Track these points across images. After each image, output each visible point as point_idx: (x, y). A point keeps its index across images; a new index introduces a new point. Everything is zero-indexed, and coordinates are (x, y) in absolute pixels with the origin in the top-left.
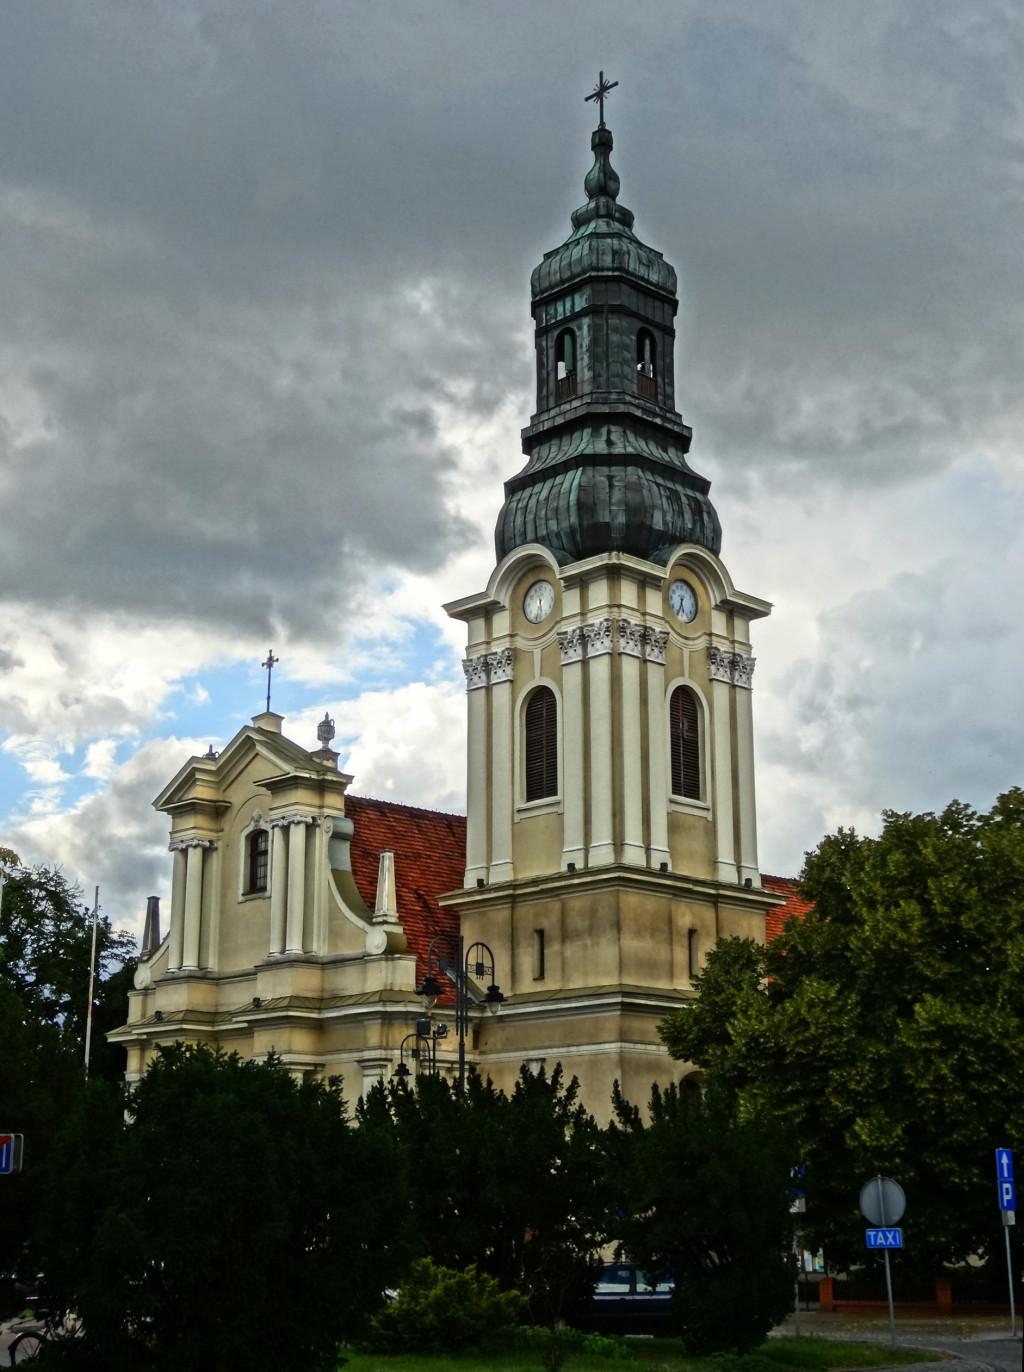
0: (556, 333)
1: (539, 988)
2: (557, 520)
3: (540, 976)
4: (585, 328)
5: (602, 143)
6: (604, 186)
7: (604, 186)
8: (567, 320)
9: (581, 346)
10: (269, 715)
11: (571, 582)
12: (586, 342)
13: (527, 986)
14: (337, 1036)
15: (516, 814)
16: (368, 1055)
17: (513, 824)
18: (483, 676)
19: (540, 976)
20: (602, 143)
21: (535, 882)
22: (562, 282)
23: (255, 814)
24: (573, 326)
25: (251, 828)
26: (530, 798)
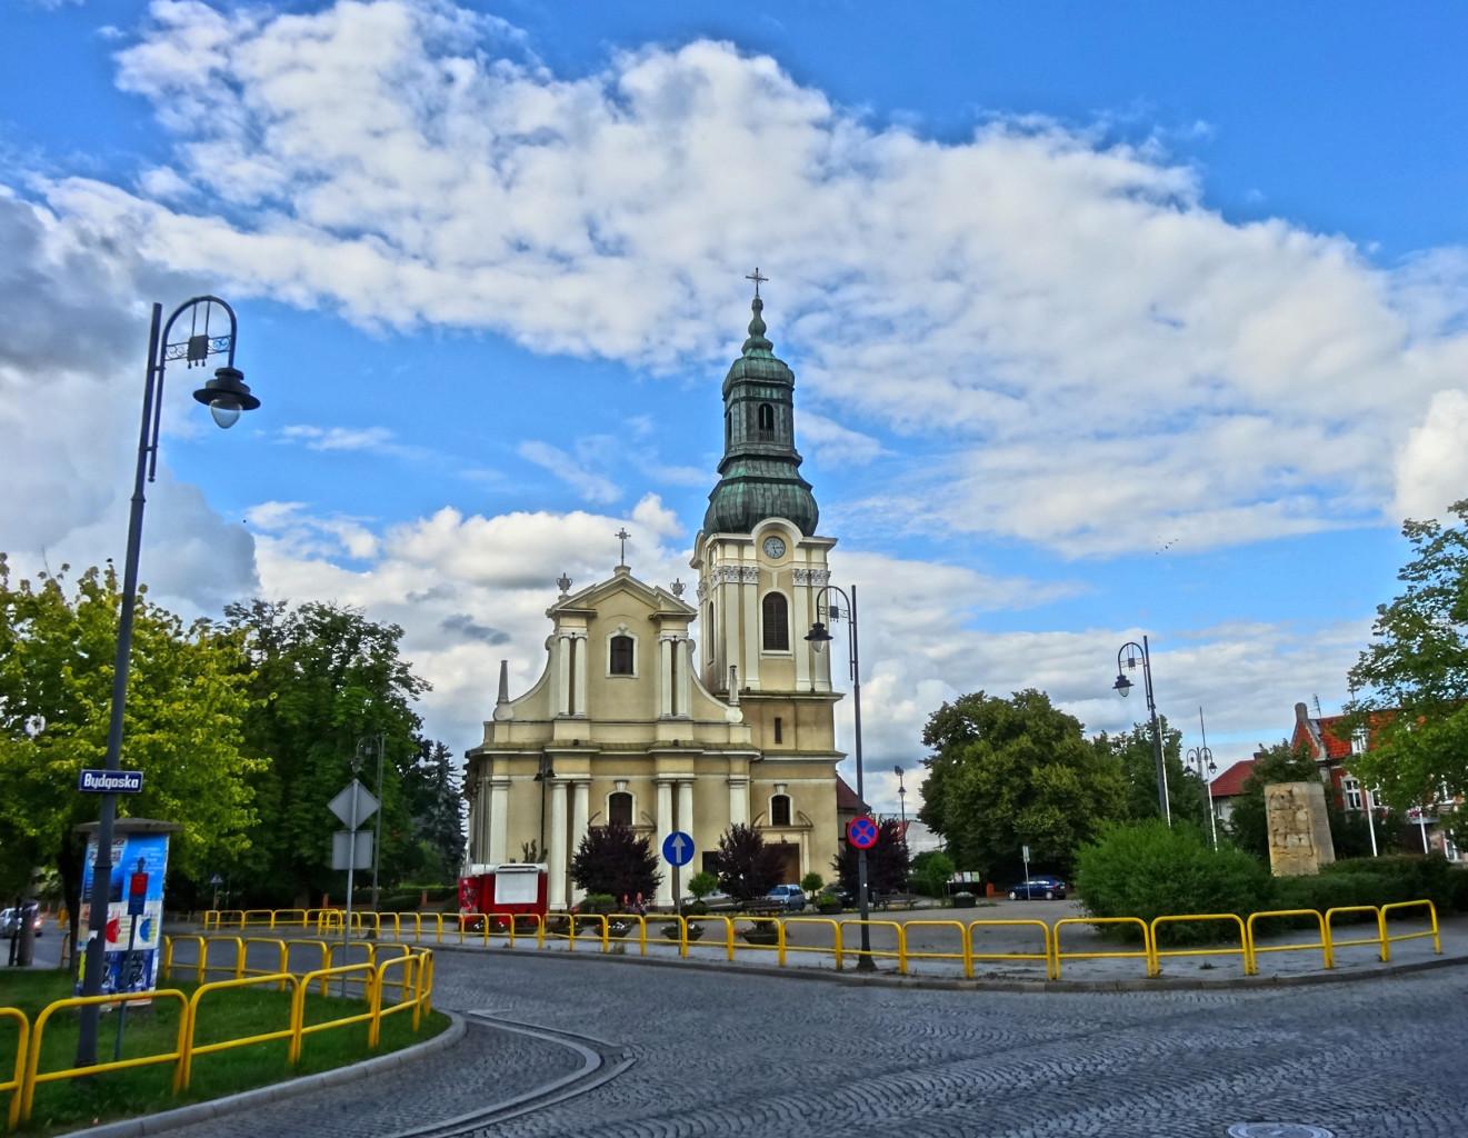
0: (760, 403)
1: (779, 747)
3: (778, 739)
5: (758, 306)
6: (758, 328)
7: (758, 328)
8: (766, 399)
10: (623, 567)
11: (801, 545)
12: (781, 417)
13: (770, 745)
14: (704, 765)
19: (778, 739)
20: (758, 306)
21: (788, 695)
23: (623, 626)
24: (773, 405)
25: (617, 633)
26: (765, 648)
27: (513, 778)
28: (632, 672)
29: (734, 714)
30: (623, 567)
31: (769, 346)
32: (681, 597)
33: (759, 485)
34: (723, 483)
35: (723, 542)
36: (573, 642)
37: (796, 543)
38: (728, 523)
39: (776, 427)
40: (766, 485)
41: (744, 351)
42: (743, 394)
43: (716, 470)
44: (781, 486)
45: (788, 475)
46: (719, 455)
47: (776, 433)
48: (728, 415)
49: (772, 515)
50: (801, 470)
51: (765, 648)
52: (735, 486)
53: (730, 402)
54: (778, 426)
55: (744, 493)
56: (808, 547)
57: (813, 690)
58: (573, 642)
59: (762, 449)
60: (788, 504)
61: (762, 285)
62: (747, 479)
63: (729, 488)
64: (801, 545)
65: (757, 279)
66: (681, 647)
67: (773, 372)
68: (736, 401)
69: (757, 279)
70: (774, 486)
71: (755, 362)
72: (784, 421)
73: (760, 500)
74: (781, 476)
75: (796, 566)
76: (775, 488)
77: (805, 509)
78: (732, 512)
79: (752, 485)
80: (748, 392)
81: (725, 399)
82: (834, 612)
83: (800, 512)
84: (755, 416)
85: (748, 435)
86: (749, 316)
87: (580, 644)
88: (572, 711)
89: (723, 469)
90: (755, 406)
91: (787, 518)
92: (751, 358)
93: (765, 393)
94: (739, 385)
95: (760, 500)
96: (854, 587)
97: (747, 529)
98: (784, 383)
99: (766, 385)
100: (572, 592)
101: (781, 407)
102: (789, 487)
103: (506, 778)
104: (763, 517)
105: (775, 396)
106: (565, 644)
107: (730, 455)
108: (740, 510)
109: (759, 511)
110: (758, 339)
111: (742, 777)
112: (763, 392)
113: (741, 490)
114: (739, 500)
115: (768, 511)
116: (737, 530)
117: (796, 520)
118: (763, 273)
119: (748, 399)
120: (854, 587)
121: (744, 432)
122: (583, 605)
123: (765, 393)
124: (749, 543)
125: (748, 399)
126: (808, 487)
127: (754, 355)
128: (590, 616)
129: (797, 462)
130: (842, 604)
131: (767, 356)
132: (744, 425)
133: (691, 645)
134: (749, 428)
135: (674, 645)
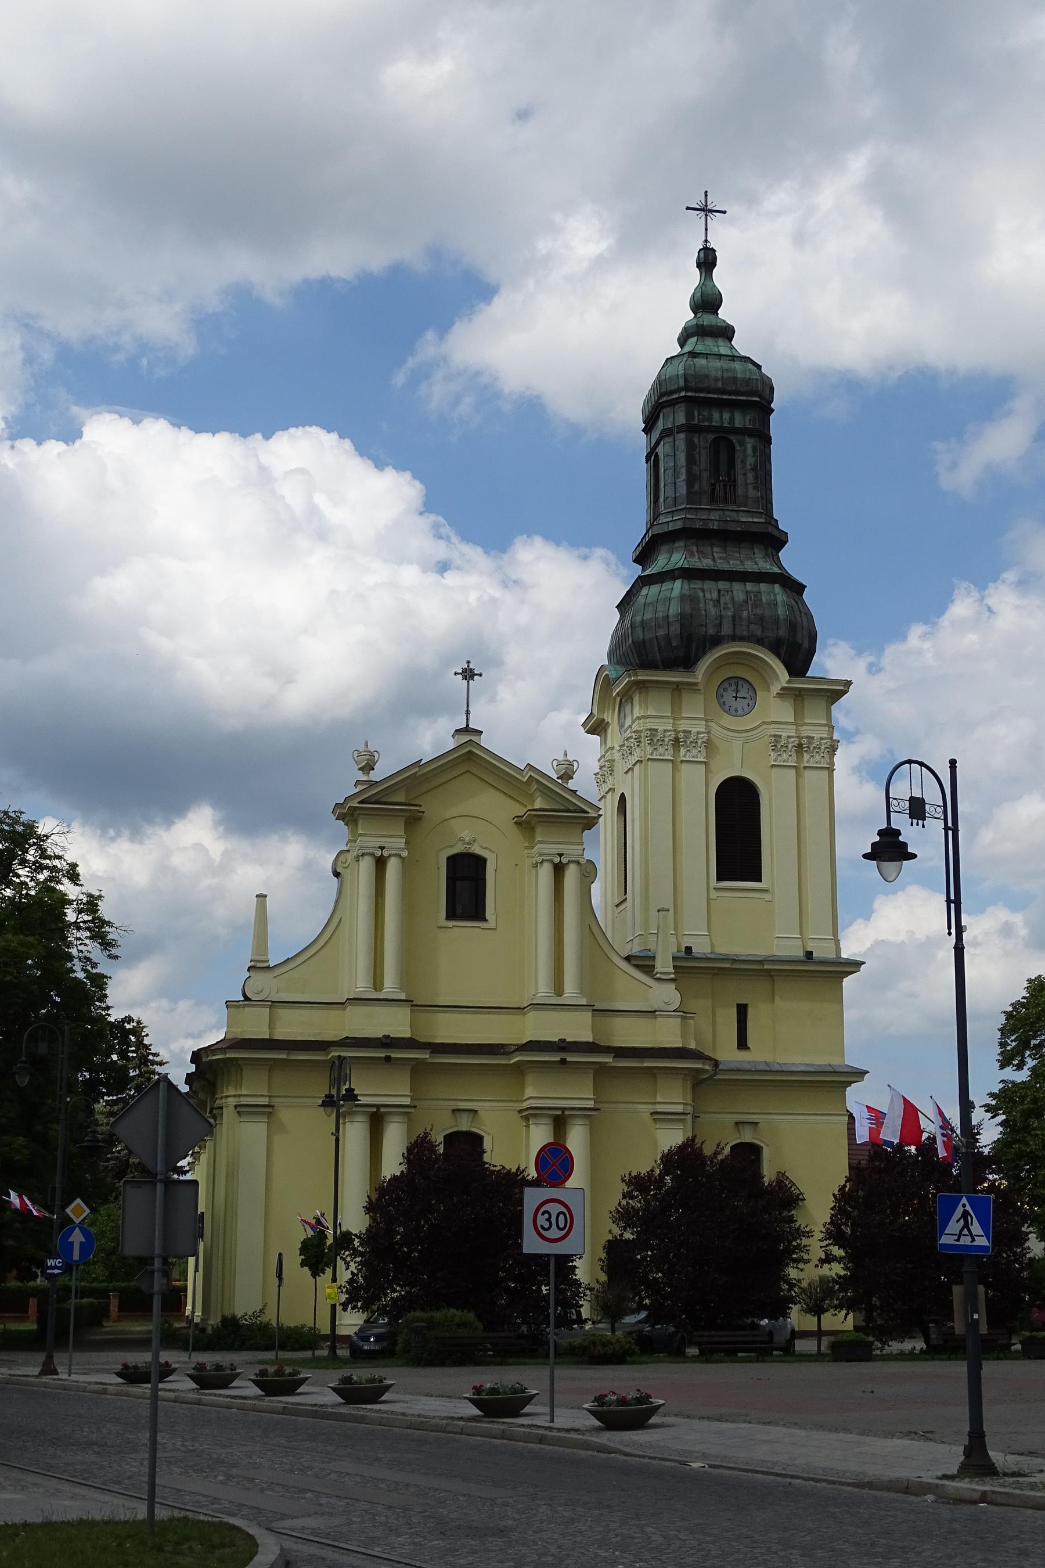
0: (711, 437)
2: (763, 627)
3: (742, 1043)
4: (749, 446)
5: (707, 261)
6: (707, 302)
7: (707, 302)
8: (720, 429)
9: (743, 462)
10: (467, 730)
11: (786, 693)
12: (750, 461)
15: (714, 894)
16: (660, 1108)
18: (670, 748)
19: (742, 1043)
20: (707, 261)
21: (761, 962)
22: (723, 392)
24: (733, 438)
27: (276, 1101)
28: (483, 919)
29: (666, 995)
30: (467, 730)
31: (727, 333)
32: (571, 785)
33: (709, 585)
34: (642, 582)
35: (642, 686)
36: (381, 863)
37: (775, 689)
38: (652, 654)
39: (740, 479)
40: (722, 585)
41: (682, 341)
42: (681, 419)
43: (631, 557)
44: (749, 586)
45: (766, 566)
46: (637, 530)
47: (740, 491)
48: (652, 457)
49: (734, 638)
50: (785, 555)
51: (719, 878)
52: (667, 586)
53: (656, 434)
54: (744, 479)
55: (682, 597)
56: (797, 697)
57: (809, 955)
58: (381, 863)
59: (713, 518)
60: (762, 618)
61: (715, 221)
62: (687, 574)
63: (655, 589)
64: (786, 693)
65: (706, 210)
66: (571, 875)
67: (735, 379)
68: (666, 433)
70: (737, 586)
71: (702, 361)
72: (754, 469)
73: (713, 611)
74: (749, 566)
75: (773, 730)
76: (739, 591)
77: (793, 626)
78: (661, 633)
79: (697, 584)
80: (689, 416)
81: (647, 430)
82: (917, 809)
83: (783, 632)
84: (704, 459)
85: (689, 493)
86: (694, 277)
87: (393, 868)
88: (377, 982)
89: (643, 557)
90: (703, 442)
91: (760, 642)
92: (693, 354)
93: (720, 418)
94: (672, 403)
95: (713, 611)
96: (953, 763)
97: (688, 663)
99: (721, 404)
100: (376, 775)
101: (750, 443)
102: (763, 587)
103: (265, 1101)
104: (716, 641)
105: (739, 422)
106: (366, 866)
107: (656, 530)
108: (675, 629)
109: (711, 631)
110: (707, 319)
111: (679, 1108)
112: (716, 415)
113: (676, 592)
114: (674, 609)
115: (727, 630)
116: (669, 664)
117: (775, 648)
118: (714, 203)
119: (690, 429)
120: (953, 763)
121: (683, 489)
122: (401, 797)
123: (720, 418)
124: (692, 687)
125: (690, 429)
126: (796, 588)
127: (700, 348)
128: (413, 821)
129: (775, 541)
130: (932, 796)
131: (724, 351)
132: (683, 476)
133: (588, 872)
134: (691, 481)
135: (559, 870)
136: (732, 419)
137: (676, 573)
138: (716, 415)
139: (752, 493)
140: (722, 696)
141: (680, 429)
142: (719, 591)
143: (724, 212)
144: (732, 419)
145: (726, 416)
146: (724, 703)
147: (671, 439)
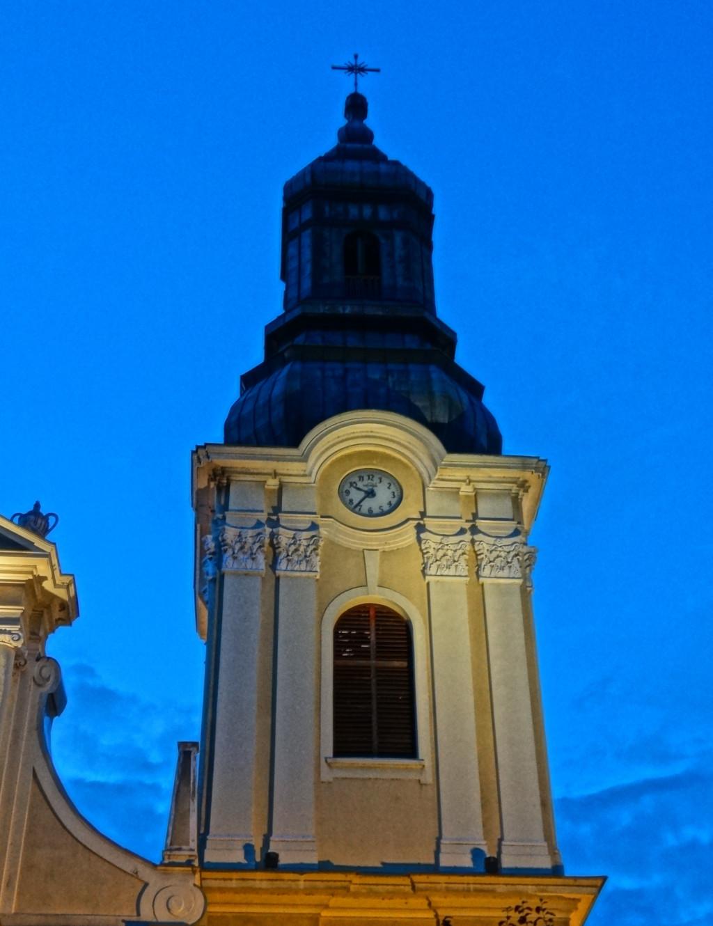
5: (356, 106)
6: (356, 139)
12: (399, 252)
17: (318, 782)
20: (356, 106)
26: (341, 749)
65: (356, 69)
69: (356, 69)
98: (410, 205)
105: (383, 214)
108: (278, 411)
118: (364, 60)
121: (307, 284)
132: (308, 269)
136: (375, 213)
137: (286, 355)
138: (353, 211)
139: (400, 281)
140: (348, 492)
141: (304, 226)
142: (346, 371)
143: (378, 71)
144: (375, 213)
145: (367, 212)
146: (351, 501)
147: (296, 241)
